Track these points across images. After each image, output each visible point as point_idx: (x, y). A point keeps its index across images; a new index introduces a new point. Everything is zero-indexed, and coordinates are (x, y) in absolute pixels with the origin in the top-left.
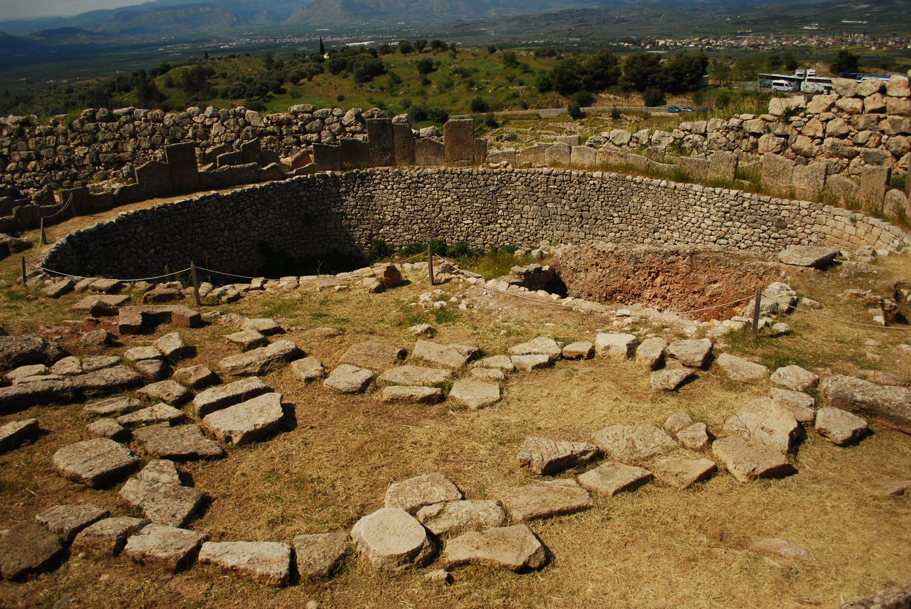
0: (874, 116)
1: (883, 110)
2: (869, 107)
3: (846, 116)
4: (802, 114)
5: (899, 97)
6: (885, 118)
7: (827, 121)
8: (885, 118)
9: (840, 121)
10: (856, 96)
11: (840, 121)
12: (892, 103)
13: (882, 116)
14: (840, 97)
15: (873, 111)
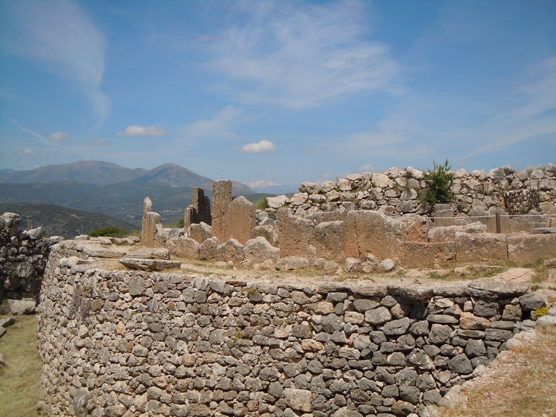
0: (335, 203)
1: (338, 199)
2: (331, 198)
3: (318, 205)
4: (291, 206)
5: (346, 191)
6: (341, 204)
7: (307, 209)
8: (341, 204)
9: (316, 208)
10: (321, 193)
11: (316, 208)
12: (344, 194)
13: (339, 202)
14: (309, 194)
15: (332, 201)
